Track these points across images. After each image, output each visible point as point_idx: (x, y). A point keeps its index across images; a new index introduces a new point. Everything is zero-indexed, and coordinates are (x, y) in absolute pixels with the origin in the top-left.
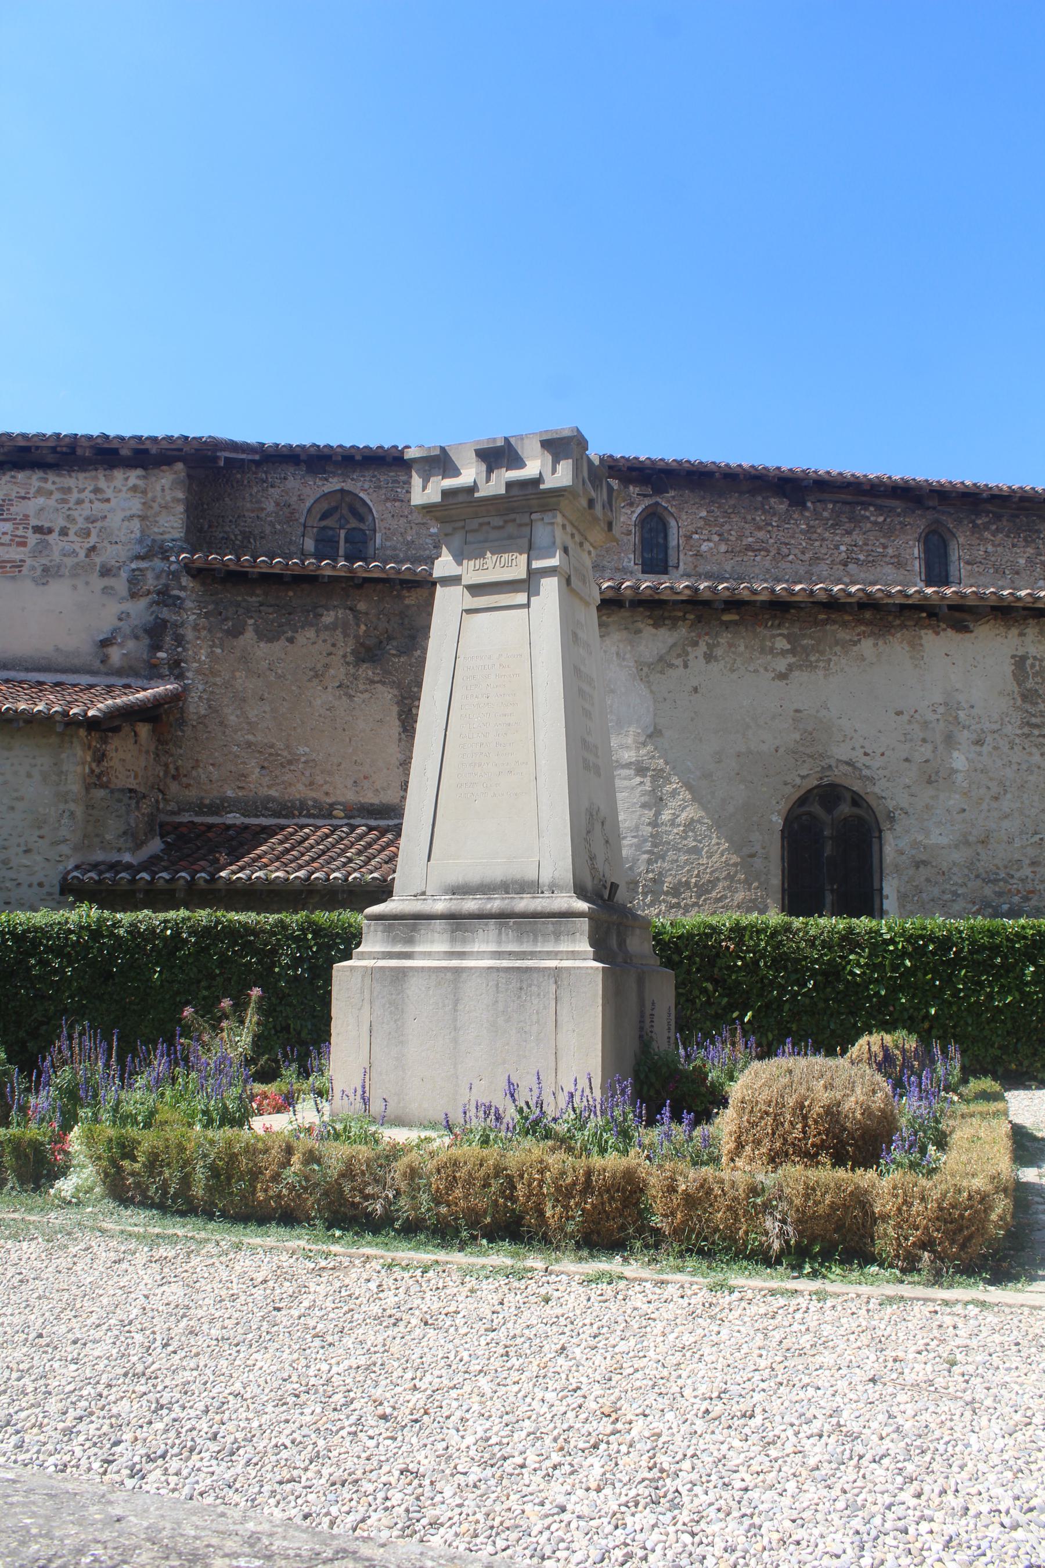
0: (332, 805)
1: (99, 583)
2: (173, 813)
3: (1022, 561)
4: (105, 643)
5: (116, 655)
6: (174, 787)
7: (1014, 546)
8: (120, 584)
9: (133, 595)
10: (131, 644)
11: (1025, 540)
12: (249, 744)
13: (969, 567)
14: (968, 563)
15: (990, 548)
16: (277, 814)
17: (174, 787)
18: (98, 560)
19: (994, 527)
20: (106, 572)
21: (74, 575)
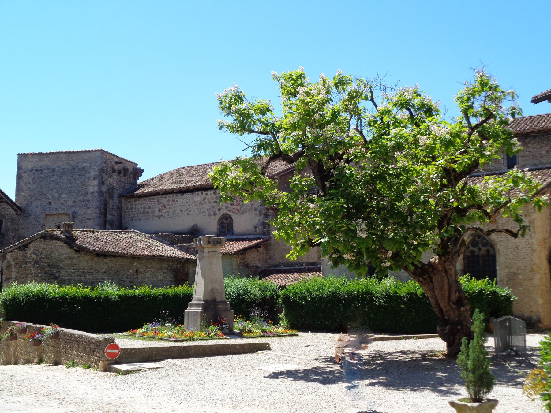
0: (303, 263)
1: (254, 213)
2: (269, 267)
3: (544, 152)
4: (256, 227)
5: (258, 230)
6: (270, 261)
7: (541, 147)
8: (258, 212)
9: (260, 215)
10: (260, 227)
11: (546, 144)
12: (285, 249)
13: (523, 158)
14: (522, 157)
15: (531, 150)
16: (291, 266)
17: (270, 261)
18: (254, 207)
19: (533, 142)
20: (255, 210)
21: (249, 211)
